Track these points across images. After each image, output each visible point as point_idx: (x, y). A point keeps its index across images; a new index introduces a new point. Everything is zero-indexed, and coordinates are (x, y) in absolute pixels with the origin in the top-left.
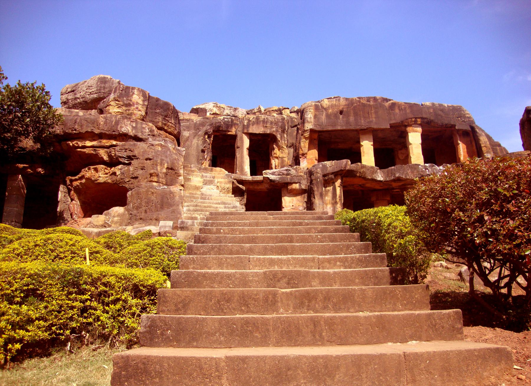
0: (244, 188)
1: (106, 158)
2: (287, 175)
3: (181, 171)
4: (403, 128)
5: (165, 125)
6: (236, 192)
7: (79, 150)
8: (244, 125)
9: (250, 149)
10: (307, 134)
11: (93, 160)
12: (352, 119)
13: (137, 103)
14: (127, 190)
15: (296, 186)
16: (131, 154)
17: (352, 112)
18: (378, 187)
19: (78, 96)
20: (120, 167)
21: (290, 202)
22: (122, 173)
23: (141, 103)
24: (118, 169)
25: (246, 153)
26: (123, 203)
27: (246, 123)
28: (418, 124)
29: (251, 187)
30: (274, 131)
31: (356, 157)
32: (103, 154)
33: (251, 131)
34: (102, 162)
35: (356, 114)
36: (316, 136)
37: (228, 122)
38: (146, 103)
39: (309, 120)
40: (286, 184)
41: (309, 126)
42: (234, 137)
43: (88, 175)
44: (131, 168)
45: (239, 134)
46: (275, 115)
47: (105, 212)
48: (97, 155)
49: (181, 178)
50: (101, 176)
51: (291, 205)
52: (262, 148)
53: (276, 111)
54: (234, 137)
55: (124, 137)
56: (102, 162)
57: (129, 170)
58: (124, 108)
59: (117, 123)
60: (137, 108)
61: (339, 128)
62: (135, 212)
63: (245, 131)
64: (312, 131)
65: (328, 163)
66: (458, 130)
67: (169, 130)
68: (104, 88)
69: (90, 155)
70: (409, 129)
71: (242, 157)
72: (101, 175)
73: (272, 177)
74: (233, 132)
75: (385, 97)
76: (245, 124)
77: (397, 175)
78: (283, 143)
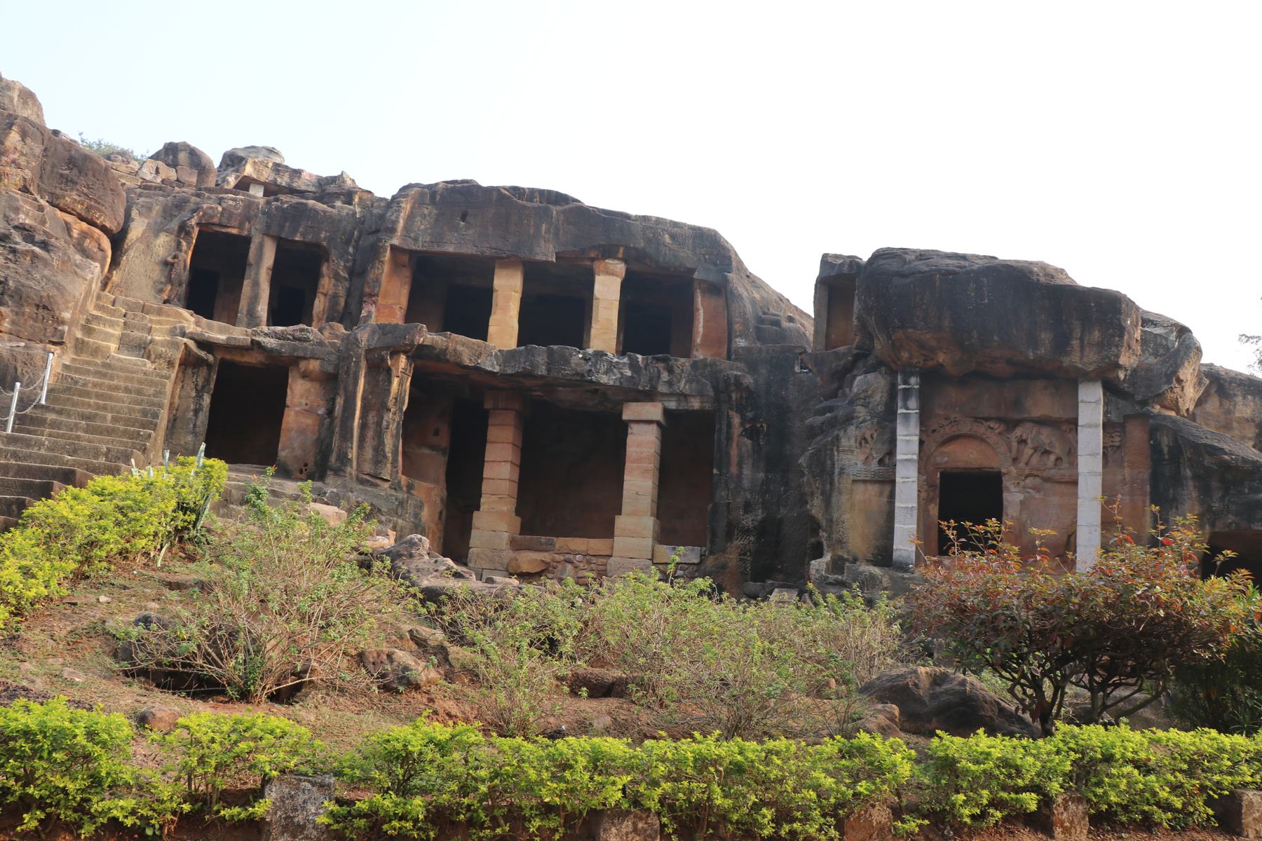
0: (211, 358)
4: (588, 263)
15: (314, 365)
21: (302, 396)
28: (619, 259)
29: (228, 357)
40: (295, 360)
42: (247, 241)
46: (338, 204)
51: (304, 401)
61: (450, 249)
66: (702, 281)
70: (598, 266)
71: (256, 284)
73: (270, 342)
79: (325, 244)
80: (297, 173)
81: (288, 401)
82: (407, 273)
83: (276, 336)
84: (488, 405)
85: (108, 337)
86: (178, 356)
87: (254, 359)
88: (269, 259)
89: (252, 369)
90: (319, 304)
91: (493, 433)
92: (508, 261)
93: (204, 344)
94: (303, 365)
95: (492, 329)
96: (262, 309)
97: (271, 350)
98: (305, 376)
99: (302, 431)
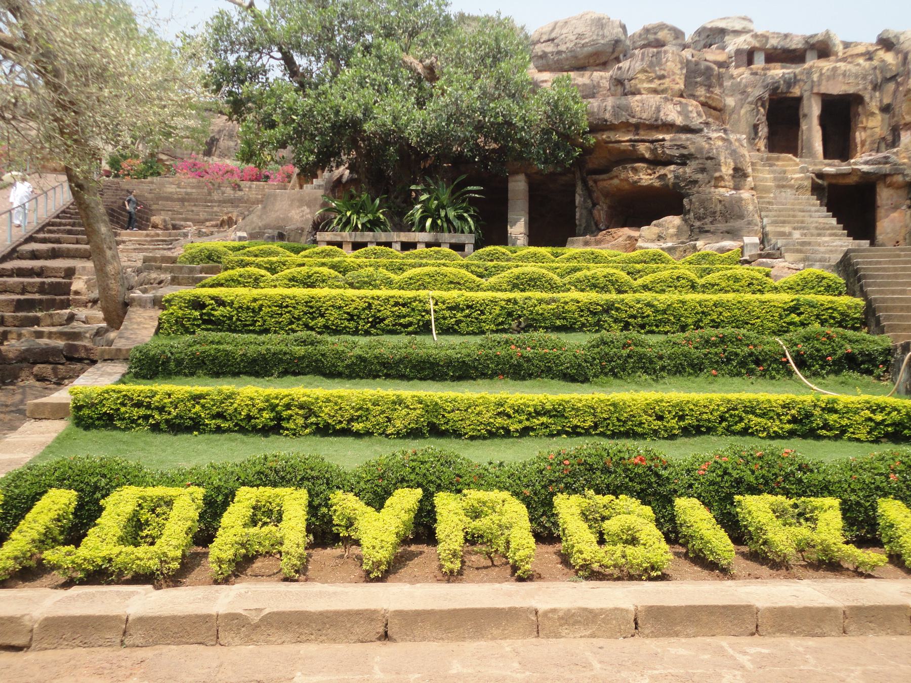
1: (647, 155)
2: (886, 163)
3: (750, 170)
5: (709, 98)
6: (816, 189)
7: (611, 145)
8: (813, 81)
11: (631, 158)
13: (674, 74)
14: (682, 196)
16: (685, 152)
19: (563, 48)
20: (672, 167)
21: (888, 199)
22: (676, 177)
23: (678, 72)
24: (670, 171)
26: (678, 210)
27: (815, 77)
29: (834, 181)
30: (860, 90)
32: (642, 148)
33: (823, 90)
34: (642, 159)
37: (790, 79)
38: (684, 71)
42: (799, 100)
43: (623, 176)
44: (688, 170)
45: (806, 95)
46: (861, 61)
47: (654, 222)
48: (635, 150)
49: (750, 179)
50: (642, 177)
51: (890, 202)
52: (840, 115)
53: (862, 55)
54: (799, 100)
55: (669, 127)
56: (642, 159)
57: (685, 172)
58: (657, 82)
59: (658, 110)
60: (674, 80)
62: (697, 224)
63: (815, 91)
67: (714, 104)
68: (603, 36)
69: (624, 151)
71: (810, 129)
72: (646, 177)
73: (865, 168)
74: (796, 91)
76: (815, 79)
78: (873, 105)
79: (860, 93)
80: (786, 36)
81: (879, 202)
83: (866, 163)
85: (766, 180)
86: (808, 183)
89: (847, 187)
90: (859, 136)
93: (820, 175)
94: (888, 180)
96: (818, 146)
98: (890, 186)
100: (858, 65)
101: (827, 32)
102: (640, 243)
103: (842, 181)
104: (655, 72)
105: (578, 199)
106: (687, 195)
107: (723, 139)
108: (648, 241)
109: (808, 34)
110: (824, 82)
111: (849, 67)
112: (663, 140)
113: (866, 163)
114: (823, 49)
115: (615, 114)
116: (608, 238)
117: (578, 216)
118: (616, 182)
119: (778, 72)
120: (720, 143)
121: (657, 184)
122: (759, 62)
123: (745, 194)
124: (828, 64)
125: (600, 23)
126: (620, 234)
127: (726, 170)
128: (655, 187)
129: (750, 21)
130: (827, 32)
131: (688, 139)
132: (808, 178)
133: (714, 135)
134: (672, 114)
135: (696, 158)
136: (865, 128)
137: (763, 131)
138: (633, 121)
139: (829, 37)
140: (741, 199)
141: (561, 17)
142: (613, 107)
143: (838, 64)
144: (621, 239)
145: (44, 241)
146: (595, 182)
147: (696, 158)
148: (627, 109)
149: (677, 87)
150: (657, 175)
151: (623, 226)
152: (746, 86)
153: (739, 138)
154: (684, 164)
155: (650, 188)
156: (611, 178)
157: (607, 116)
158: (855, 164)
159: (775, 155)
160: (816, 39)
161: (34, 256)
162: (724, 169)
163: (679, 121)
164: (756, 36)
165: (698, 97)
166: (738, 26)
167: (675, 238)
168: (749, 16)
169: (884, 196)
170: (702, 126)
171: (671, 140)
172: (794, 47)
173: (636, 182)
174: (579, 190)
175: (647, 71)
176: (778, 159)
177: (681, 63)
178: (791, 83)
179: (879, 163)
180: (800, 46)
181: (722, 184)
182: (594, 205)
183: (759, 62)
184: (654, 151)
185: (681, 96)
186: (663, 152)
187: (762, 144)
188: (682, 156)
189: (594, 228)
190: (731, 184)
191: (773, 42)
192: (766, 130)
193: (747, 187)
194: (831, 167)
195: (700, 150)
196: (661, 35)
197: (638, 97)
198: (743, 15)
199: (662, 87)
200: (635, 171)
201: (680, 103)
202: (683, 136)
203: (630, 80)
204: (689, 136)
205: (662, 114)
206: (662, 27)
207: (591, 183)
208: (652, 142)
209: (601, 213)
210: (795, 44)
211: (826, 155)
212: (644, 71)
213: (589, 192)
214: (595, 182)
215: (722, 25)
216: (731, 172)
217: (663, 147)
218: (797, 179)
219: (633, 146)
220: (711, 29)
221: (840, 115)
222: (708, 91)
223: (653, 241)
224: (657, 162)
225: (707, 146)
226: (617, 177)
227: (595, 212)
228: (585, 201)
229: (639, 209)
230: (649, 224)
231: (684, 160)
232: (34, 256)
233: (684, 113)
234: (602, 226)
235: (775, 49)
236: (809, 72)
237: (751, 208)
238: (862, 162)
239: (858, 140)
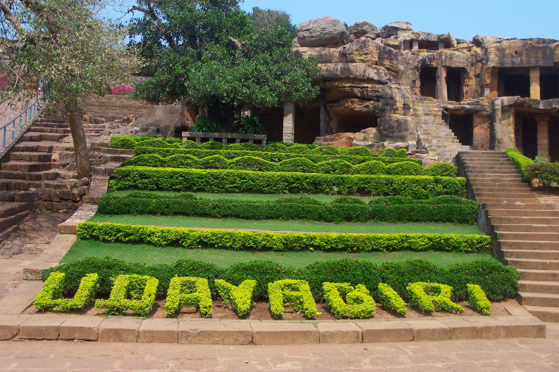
1: (359, 95)
2: (477, 105)
3: (411, 105)
8: (442, 60)
9: (447, 78)
10: (490, 70)
12: (524, 58)
13: (373, 52)
14: (376, 118)
16: (379, 94)
17: (525, 52)
18: (540, 112)
19: (314, 34)
20: (372, 102)
22: (374, 107)
23: (375, 52)
25: (444, 81)
27: (443, 58)
29: (453, 112)
31: (526, 93)
32: (356, 91)
33: (447, 65)
34: (356, 97)
35: (528, 55)
36: (497, 71)
38: (378, 52)
39: (491, 59)
40: (476, 112)
41: (491, 64)
42: (436, 68)
44: (380, 104)
46: (465, 51)
47: (362, 131)
48: (352, 92)
49: (412, 110)
52: (456, 77)
53: (466, 48)
54: (436, 68)
55: (370, 80)
56: (356, 97)
57: (379, 105)
59: (365, 71)
60: (373, 56)
63: (443, 65)
64: (493, 67)
65: (505, 98)
69: (347, 92)
71: (441, 84)
72: (358, 106)
74: (434, 64)
75: (552, 38)
77: (554, 106)
78: (472, 74)
80: (429, 34)
82: (497, 75)
84: (537, 119)
86: (440, 113)
87: (462, 113)
88: (444, 74)
90: (465, 89)
91: (539, 129)
92: (534, 68)
93: (446, 109)
94: (479, 113)
95: (531, 92)
97: (469, 109)
98: (479, 116)
99: (481, 134)
100: (464, 53)
101: (449, 34)
102: (355, 142)
103: (457, 113)
104: (363, 51)
105: (322, 116)
106: (380, 117)
107: (398, 88)
108: (358, 140)
109: (440, 34)
110: (448, 61)
111: (460, 54)
112: (367, 87)
113: (468, 104)
114: (446, 42)
115: (342, 72)
116: (338, 138)
117: (321, 125)
118: (342, 108)
119: (424, 54)
120: (396, 90)
121: (364, 110)
122: (416, 48)
123: (409, 118)
124: (449, 51)
125: (335, 23)
126: (344, 136)
127: (399, 105)
128: (363, 112)
129: (411, 24)
130: (449, 34)
131: (380, 88)
132: (439, 111)
133: (393, 86)
134: (372, 73)
135: (384, 98)
136: (468, 85)
137: (418, 84)
138: (351, 76)
139: (450, 37)
140: (406, 121)
141: (314, 18)
142: (341, 68)
143: (455, 52)
144: (344, 139)
145: (35, 131)
146: (331, 107)
147: (384, 98)
148: (348, 70)
149: (374, 59)
150: (364, 105)
151: (345, 132)
152: (409, 60)
153: (406, 88)
154: (378, 101)
155: (360, 112)
156: (339, 106)
157: (338, 73)
158: (463, 104)
159: (424, 97)
160: (443, 37)
161: (31, 139)
162: (398, 104)
163: (376, 78)
164: (413, 33)
165: (385, 65)
166: (404, 27)
167: (373, 140)
168: (410, 22)
169: (476, 120)
170: (387, 81)
171: (372, 88)
172: (433, 40)
173: (353, 109)
174: (322, 111)
175: (359, 51)
176: (425, 99)
177: (376, 47)
178: (432, 59)
179: (475, 104)
180: (435, 40)
181: (398, 112)
182: (330, 120)
183: (416, 48)
184: (362, 93)
185: (376, 64)
186: (367, 94)
187: (417, 90)
188: (377, 96)
189: (330, 132)
190: (402, 112)
191: (422, 37)
192: (419, 83)
193: (410, 114)
194: (452, 106)
195: (387, 94)
196: (365, 28)
197: (354, 64)
198: (406, 21)
199: (367, 59)
200: (352, 102)
201: (376, 68)
202: (378, 86)
203: (350, 55)
204: (381, 86)
205: (366, 74)
206: (365, 24)
207: (328, 108)
208: (361, 88)
209: (334, 124)
210: (433, 39)
211: (449, 98)
212: (357, 50)
213: (327, 112)
214: (331, 107)
215: (396, 25)
216: (402, 106)
217: (367, 91)
218: (435, 111)
219: (352, 90)
220: (391, 27)
221: (456, 77)
222: (390, 62)
223: (361, 140)
224: (364, 98)
225: (390, 92)
226: (342, 105)
227: (331, 123)
228: (325, 117)
229: (355, 123)
230: (359, 131)
231: (378, 98)
232: (31, 139)
233: (378, 73)
234: (334, 131)
235: (423, 40)
236: (440, 55)
237: (412, 125)
238: (466, 103)
239: (464, 91)
